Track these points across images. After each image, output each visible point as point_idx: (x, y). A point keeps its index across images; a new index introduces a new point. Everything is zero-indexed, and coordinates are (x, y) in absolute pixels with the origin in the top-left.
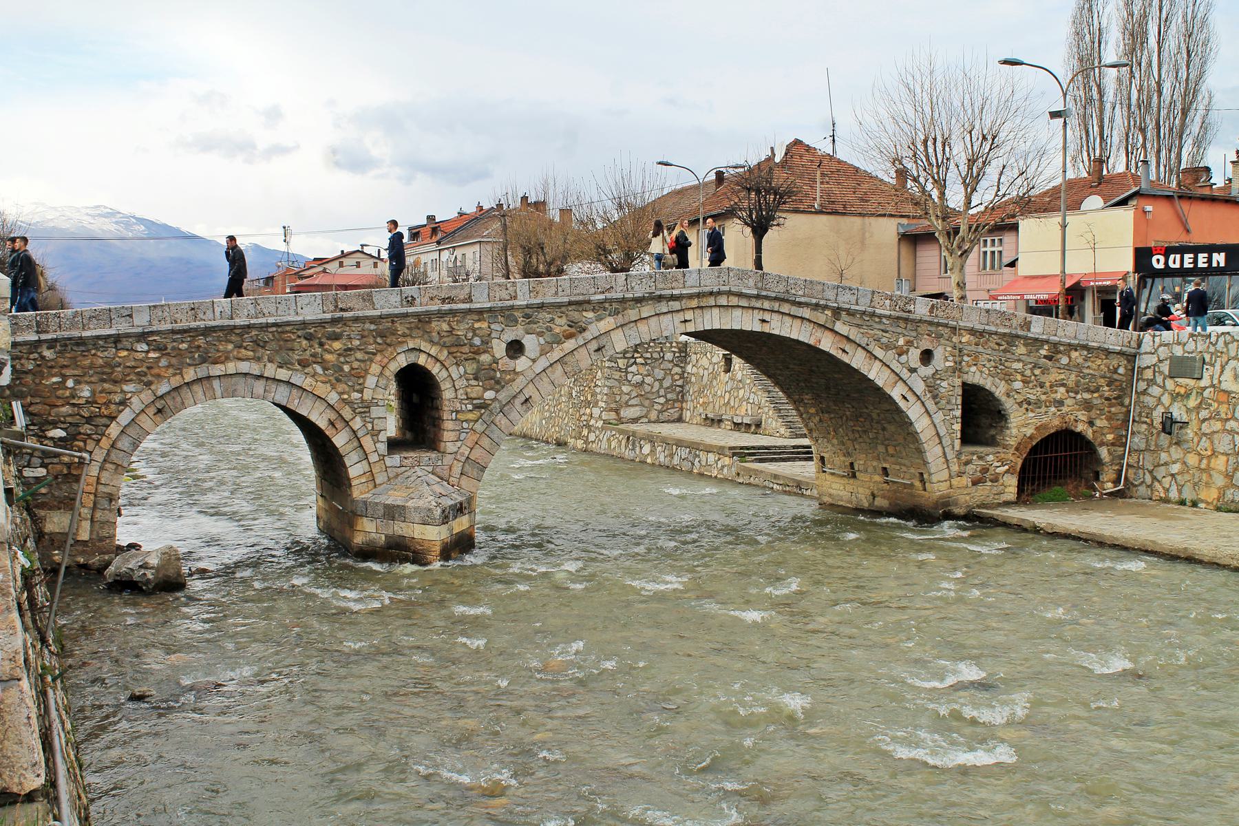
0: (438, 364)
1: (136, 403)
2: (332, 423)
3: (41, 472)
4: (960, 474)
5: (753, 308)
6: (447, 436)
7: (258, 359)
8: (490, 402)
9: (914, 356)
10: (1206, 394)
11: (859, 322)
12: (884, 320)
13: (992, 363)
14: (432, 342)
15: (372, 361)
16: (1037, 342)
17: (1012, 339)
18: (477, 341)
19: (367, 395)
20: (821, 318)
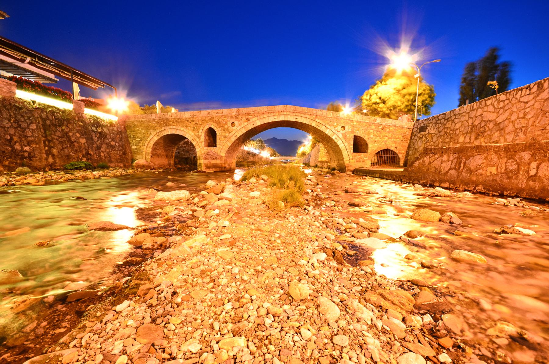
1: (153, 134)
3: (135, 147)
9: (339, 128)
16: (378, 125)
17: (370, 124)
18: (224, 123)
19: (200, 134)
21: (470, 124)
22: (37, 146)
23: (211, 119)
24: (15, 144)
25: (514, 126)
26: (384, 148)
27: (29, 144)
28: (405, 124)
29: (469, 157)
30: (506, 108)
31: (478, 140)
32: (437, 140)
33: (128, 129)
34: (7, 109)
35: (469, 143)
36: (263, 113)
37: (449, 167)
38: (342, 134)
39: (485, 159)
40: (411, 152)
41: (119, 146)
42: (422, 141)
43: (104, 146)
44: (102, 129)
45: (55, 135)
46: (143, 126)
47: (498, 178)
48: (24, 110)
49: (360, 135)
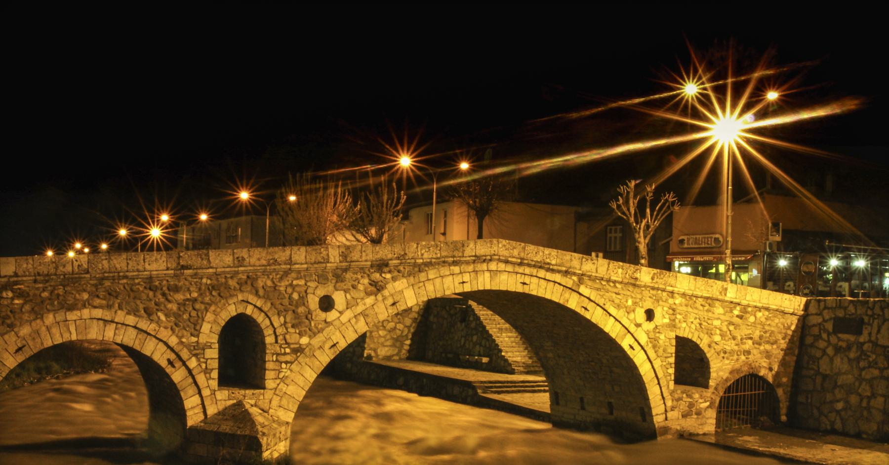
0: (263, 314)
2: (170, 363)
4: (673, 409)
5: (517, 273)
6: (269, 375)
7: (109, 307)
8: (305, 347)
10: (865, 347)
11: (600, 286)
12: (617, 285)
13: (698, 320)
14: (259, 297)
15: (207, 310)
16: (734, 304)
17: (710, 300)
18: (295, 296)
19: (203, 339)
20: (570, 284)
23: (250, 281)
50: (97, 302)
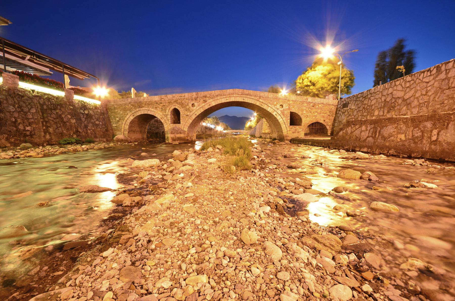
1: (129, 115)
3: (115, 125)
9: (278, 106)
16: (310, 103)
18: (186, 104)
19: (167, 113)
21: (383, 100)
22: (37, 126)
23: (176, 101)
24: (19, 125)
25: (418, 101)
26: (314, 121)
27: (30, 124)
28: (331, 102)
29: (383, 127)
30: (412, 87)
31: (390, 114)
32: (357, 114)
33: (110, 111)
34: (12, 97)
35: (383, 115)
36: (217, 96)
37: (367, 135)
38: (281, 111)
39: (396, 128)
40: (336, 124)
41: (102, 125)
42: (345, 115)
43: (90, 125)
44: (89, 112)
45: (51, 117)
46: (121, 108)
47: (406, 143)
48: (26, 98)
49: (295, 112)
50: (146, 106)
